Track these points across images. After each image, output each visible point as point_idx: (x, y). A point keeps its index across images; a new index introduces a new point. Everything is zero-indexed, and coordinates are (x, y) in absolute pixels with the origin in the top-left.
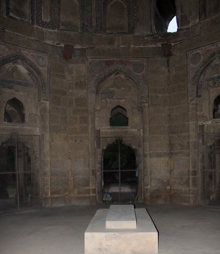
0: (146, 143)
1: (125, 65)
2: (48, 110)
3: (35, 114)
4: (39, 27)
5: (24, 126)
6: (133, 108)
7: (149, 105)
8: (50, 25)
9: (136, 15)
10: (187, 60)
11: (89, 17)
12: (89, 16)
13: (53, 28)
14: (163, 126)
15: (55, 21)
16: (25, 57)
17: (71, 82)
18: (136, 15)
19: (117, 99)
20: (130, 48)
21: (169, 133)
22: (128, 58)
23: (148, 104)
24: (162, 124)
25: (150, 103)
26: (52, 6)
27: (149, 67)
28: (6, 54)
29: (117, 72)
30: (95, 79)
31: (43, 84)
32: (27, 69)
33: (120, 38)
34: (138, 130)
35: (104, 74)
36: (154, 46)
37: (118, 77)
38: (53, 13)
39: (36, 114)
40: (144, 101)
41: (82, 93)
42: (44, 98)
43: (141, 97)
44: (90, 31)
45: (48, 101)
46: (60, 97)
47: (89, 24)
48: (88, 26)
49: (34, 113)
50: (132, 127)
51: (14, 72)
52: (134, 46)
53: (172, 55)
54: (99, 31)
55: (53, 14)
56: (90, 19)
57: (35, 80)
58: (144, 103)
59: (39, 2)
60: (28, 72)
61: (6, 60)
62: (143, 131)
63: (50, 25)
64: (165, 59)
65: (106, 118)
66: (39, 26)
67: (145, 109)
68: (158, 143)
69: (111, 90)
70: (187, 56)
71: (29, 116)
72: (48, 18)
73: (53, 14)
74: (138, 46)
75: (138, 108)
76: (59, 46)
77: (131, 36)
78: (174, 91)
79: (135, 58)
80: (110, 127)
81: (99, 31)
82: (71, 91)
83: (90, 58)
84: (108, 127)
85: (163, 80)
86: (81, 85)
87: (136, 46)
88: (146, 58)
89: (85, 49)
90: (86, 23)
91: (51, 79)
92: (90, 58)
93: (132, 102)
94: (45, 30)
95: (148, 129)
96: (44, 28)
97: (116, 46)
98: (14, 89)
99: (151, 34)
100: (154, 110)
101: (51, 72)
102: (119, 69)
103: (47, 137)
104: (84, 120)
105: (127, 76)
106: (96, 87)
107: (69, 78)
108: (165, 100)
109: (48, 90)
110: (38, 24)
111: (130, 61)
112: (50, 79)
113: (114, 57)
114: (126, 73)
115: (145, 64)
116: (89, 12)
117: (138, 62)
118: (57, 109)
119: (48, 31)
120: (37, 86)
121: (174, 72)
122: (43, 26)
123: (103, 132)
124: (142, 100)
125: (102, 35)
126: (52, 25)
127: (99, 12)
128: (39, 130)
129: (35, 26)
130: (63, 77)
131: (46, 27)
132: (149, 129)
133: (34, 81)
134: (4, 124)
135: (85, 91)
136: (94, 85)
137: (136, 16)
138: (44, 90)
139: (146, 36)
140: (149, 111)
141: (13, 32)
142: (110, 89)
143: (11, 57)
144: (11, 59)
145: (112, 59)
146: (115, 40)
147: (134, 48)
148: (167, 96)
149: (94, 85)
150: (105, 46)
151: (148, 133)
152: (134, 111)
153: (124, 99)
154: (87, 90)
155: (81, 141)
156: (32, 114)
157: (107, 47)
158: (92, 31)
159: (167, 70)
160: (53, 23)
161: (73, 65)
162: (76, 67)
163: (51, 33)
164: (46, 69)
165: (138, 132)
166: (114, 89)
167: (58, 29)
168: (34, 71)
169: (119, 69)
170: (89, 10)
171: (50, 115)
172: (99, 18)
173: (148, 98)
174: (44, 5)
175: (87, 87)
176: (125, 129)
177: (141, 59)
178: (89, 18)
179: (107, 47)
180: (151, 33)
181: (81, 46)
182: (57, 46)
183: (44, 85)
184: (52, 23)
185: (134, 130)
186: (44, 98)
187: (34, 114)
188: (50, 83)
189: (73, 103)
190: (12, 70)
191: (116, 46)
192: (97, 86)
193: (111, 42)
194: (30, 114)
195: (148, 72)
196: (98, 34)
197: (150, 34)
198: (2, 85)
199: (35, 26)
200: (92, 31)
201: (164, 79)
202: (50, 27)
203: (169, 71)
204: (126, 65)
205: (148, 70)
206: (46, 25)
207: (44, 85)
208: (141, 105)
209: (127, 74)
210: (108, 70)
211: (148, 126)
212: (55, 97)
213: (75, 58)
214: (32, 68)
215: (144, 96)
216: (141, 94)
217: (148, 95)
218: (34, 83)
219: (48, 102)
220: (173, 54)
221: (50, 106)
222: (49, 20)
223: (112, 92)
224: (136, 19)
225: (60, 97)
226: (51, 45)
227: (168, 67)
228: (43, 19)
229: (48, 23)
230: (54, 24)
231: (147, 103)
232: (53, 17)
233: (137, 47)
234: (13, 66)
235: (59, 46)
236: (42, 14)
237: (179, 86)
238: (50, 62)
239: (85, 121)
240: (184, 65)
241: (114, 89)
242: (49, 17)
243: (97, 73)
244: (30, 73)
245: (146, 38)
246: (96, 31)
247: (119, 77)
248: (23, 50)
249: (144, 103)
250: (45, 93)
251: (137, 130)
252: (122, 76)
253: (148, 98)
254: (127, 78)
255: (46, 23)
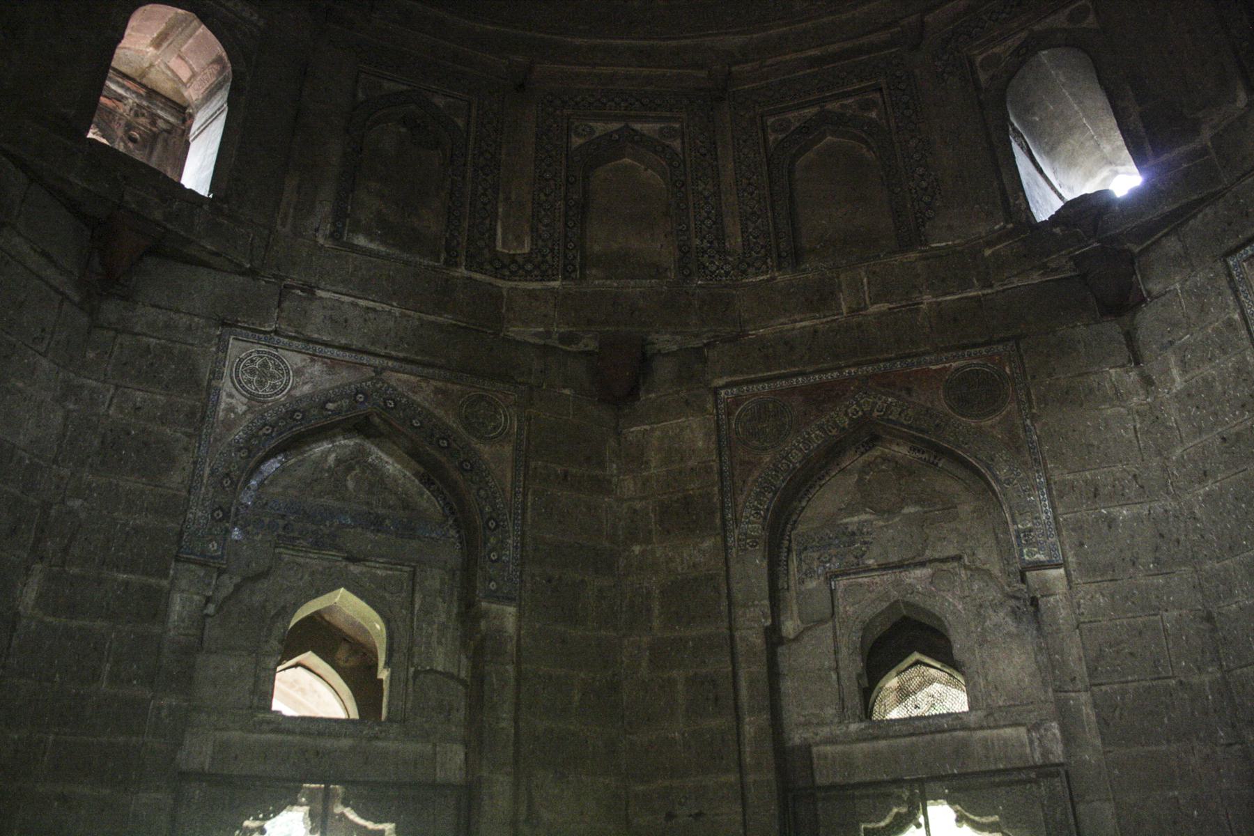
0: (1097, 804)
1: (903, 393)
2: (511, 647)
3: (451, 676)
4: (478, 276)
5: (377, 738)
6: (981, 606)
7: (1068, 574)
8: (529, 267)
9: (921, 170)
10: (1237, 297)
11: (708, 218)
12: (709, 213)
13: (544, 277)
14: (1181, 683)
15: (552, 250)
16: (404, 400)
17: (638, 505)
18: (921, 170)
19: (884, 567)
20: (918, 310)
21: (1233, 726)
22: (916, 355)
23: (1062, 571)
24: (1173, 677)
25: (1071, 559)
26: (543, 197)
27: (1034, 377)
28: (307, 389)
29: (868, 433)
30: (760, 476)
31: (489, 519)
32: (414, 454)
33: (863, 274)
34: (1029, 731)
35: (801, 450)
36: (1036, 278)
37: (879, 460)
38: (546, 221)
39: (455, 671)
40: (1041, 557)
41: (697, 552)
42: (493, 586)
43: (1018, 537)
44: (714, 268)
45: (509, 599)
46: (583, 581)
47: (711, 243)
48: (704, 252)
49: (440, 668)
50: (991, 714)
51: (350, 469)
52: (937, 296)
53: (1144, 300)
54: (758, 264)
55: (546, 226)
56: (715, 223)
57: (455, 507)
58: (1039, 566)
59: (486, 190)
60: (422, 470)
61: (303, 413)
62: (1063, 730)
63: (529, 267)
64: (1112, 329)
65: (834, 676)
66: (481, 270)
67: (1052, 599)
68: (1176, 798)
69: (850, 528)
70: (1230, 275)
71: (411, 682)
72: (522, 244)
73: (546, 226)
74: (953, 293)
75: (1013, 602)
76: (574, 348)
77: (913, 255)
78: (1205, 473)
79: (947, 349)
80: (863, 725)
81: (758, 264)
82: (637, 549)
83: (727, 386)
84: (854, 727)
85: (1126, 429)
86: (684, 514)
87: (946, 294)
88: (1009, 339)
89: (698, 350)
90: (698, 242)
91: (530, 497)
92: (727, 386)
93: (969, 573)
94: (504, 285)
95: (1088, 712)
96: (503, 277)
97: (845, 310)
98: (339, 549)
99: (1010, 226)
100: (1104, 596)
101: (533, 464)
102: (876, 414)
103: (500, 793)
104: (711, 696)
105: (922, 440)
106: (765, 518)
107: (629, 486)
108: (1162, 536)
109: (516, 547)
110: (474, 262)
111: (929, 370)
112: (525, 495)
113: (842, 363)
114: (917, 430)
115: (1007, 369)
116: (706, 198)
117: (970, 365)
118: (563, 641)
119: (524, 290)
120: (462, 532)
121: (1178, 379)
122: (497, 273)
123: (826, 758)
124: (1025, 551)
125: (773, 278)
126: (537, 267)
127: (752, 194)
128: (462, 756)
129: (462, 271)
130: (601, 486)
131: (513, 273)
132: (1098, 715)
133: (451, 508)
134: (265, 727)
135: (707, 544)
136: (756, 508)
137: (922, 176)
138: (493, 549)
139: (989, 244)
140: (1079, 606)
141: (352, 299)
142: (845, 521)
143: (329, 401)
144: (330, 406)
145: (835, 374)
146: (840, 285)
147: (939, 304)
148: (1166, 511)
149: (756, 508)
150: (795, 321)
151: (1098, 742)
152: (988, 623)
153: (922, 564)
154: (719, 539)
155: (699, 815)
156: (432, 671)
157: (803, 324)
158: (727, 268)
159: (1133, 375)
160: (544, 256)
161: (648, 427)
162: (658, 433)
163: (531, 294)
164: (508, 450)
165: (1031, 742)
166: (864, 517)
167: (564, 278)
168: (444, 459)
169: (876, 414)
170: (706, 193)
171: (520, 677)
172: (753, 213)
173: (1059, 534)
174: (507, 199)
175: (718, 521)
176: (955, 730)
177: (983, 350)
178: (709, 222)
179: (803, 324)
180: (1007, 222)
181: (678, 338)
182: (568, 353)
183: (492, 524)
184: (540, 259)
185: (1009, 732)
186: (493, 586)
187: (440, 673)
188: (524, 512)
189: (649, 610)
190: (339, 461)
191: (845, 310)
192: (768, 509)
193: (821, 297)
194: (416, 673)
195: (1029, 400)
196: (756, 275)
197: (1004, 227)
198: (280, 532)
199: (462, 271)
200: (727, 268)
201: (1130, 426)
202: (528, 273)
203: (1147, 381)
204: (909, 391)
205: (1028, 395)
206: (514, 267)
207: (492, 524)
208: (1023, 587)
209: (922, 431)
210: (821, 428)
211: (1084, 697)
212: (549, 581)
213: (653, 395)
214: (431, 443)
215: (1030, 530)
216: (1015, 523)
217: (1055, 518)
218: (451, 522)
219: (511, 610)
220: (1149, 293)
221: (519, 628)
222: (526, 250)
223: (853, 534)
224: (924, 184)
225: (583, 581)
226: (534, 345)
227: (1137, 363)
228: (499, 248)
229: (520, 260)
230: (549, 258)
231: (1058, 566)
232: (546, 236)
233: (949, 298)
234: (346, 446)
235: (574, 348)
236: (495, 230)
237: (1224, 439)
238: (529, 419)
239: (716, 699)
240: (1230, 324)
241: (864, 517)
242: (527, 240)
243: (765, 449)
244: (431, 475)
245: (988, 252)
246: (744, 266)
247: (885, 459)
248: (393, 370)
249: (1039, 566)
250: (496, 561)
251: (1023, 730)
252: (901, 451)
253: (1059, 534)
254: (925, 456)
255: (514, 262)
